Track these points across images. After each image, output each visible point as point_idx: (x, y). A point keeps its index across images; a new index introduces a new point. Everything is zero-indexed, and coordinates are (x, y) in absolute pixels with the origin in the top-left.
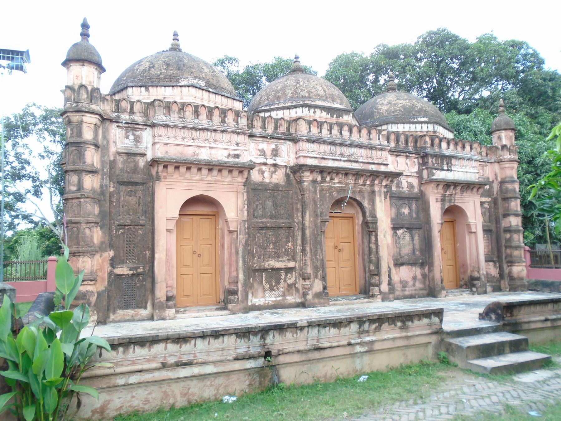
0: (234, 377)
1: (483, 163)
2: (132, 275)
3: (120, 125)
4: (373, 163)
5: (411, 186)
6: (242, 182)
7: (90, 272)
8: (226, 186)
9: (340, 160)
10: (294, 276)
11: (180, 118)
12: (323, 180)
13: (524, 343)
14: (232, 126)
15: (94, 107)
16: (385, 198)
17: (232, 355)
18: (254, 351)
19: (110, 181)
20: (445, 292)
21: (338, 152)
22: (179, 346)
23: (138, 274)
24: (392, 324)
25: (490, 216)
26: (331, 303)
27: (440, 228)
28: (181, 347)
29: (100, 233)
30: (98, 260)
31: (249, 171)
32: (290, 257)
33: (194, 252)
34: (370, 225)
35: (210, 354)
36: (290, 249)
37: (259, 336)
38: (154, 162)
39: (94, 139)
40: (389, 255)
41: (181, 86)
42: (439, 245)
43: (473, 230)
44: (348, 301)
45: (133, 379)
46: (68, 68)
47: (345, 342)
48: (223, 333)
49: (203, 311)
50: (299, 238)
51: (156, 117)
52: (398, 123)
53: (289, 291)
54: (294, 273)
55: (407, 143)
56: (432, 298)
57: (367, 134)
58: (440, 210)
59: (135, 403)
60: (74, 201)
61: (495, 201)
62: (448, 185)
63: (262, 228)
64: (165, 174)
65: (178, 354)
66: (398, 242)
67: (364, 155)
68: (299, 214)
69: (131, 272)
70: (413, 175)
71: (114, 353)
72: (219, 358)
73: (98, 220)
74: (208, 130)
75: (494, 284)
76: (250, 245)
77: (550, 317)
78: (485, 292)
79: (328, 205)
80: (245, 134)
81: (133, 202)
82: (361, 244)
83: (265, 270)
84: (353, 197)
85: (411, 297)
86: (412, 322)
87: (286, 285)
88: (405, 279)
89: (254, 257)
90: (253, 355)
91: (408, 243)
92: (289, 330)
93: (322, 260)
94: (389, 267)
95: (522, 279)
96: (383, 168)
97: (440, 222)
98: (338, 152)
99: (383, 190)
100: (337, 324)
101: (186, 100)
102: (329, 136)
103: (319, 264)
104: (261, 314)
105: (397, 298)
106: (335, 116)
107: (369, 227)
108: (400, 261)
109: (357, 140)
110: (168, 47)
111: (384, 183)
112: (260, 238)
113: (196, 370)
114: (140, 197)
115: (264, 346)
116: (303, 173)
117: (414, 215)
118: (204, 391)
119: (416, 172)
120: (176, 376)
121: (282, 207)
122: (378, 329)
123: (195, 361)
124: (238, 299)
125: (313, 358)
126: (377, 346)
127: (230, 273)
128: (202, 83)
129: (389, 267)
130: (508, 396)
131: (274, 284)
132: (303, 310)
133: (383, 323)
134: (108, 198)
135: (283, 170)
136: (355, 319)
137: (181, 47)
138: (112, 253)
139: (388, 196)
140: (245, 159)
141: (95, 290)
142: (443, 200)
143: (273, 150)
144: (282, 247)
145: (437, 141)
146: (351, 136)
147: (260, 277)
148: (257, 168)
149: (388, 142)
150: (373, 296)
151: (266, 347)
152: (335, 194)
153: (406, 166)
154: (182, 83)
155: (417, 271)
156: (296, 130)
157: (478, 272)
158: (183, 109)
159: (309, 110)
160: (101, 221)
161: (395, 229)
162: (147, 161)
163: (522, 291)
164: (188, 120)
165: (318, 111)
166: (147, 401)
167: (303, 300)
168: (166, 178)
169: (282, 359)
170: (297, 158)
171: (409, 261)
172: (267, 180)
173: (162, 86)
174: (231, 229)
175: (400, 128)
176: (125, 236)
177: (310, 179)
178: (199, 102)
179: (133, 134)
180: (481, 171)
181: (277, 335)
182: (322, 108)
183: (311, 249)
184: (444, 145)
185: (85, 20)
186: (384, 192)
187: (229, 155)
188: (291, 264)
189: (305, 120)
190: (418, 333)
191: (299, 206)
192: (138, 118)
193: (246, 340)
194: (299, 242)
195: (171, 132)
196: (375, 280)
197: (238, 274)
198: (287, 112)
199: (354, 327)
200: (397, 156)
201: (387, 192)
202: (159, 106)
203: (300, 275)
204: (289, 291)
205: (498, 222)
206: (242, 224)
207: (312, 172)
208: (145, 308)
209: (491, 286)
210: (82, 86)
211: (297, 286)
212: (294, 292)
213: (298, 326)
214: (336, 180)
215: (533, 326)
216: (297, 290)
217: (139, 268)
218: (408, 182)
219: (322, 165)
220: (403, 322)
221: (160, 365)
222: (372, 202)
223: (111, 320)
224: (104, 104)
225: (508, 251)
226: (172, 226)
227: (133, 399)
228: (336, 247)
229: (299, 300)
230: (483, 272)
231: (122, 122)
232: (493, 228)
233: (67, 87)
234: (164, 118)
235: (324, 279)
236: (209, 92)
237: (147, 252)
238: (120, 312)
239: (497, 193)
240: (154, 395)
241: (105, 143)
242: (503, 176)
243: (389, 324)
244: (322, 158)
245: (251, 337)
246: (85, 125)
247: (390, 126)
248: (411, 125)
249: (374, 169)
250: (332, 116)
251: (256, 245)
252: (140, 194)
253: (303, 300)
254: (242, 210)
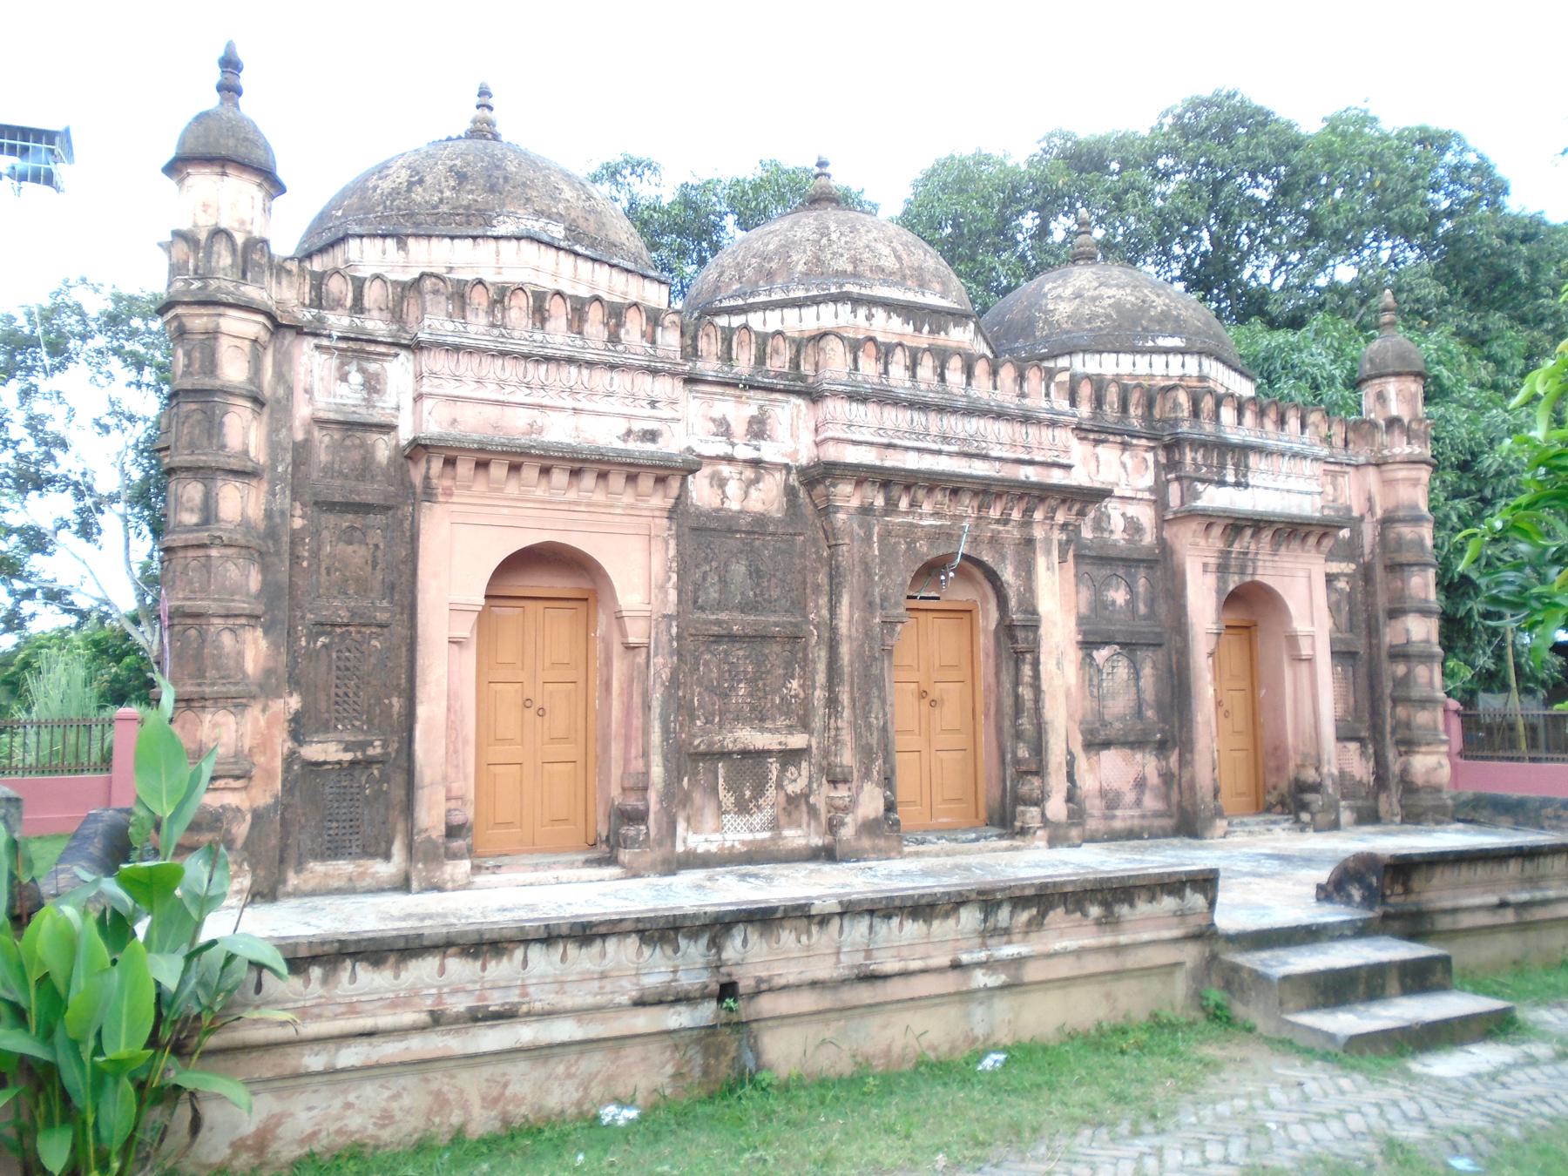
0: (632, 1053)
1: (1336, 466)
2: (353, 763)
3: (325, 342)
4: (1031, 463)
5: (1133, 526)
6: (662, 509)
7: (232, 753)
8: (618, 519)
9: (939, 452)
10: (805, 773)
11: (493, 326)
12: (891, 507)
13: (1439, 966)
14: (639, 350)
15: (251, 292)
16: (1063, 560)
17: (627, 991)
18: (691, 979)
19: (294, 499)
20: (1224, 823)
21: (934, 430)
22: (479, 964)
23: (369, 762)
24: (1074, 912)
25: (1351, 612)
26: (906, 849)
27: (1212, 646)
28: (484, 968)
29: (263, 644)
30: (256, 720)
31: (684, 479)
32: (794, 720)
33: (527, 703)
34: (1020, 634)
35: (567, 987)
36: (796, 696)
37: (704, 941)
38: (418, 449)
39: (250, 381)
40: (1070, 717)
41: (496, 238)
42: (1210, 691)
43: (1305, 651)
44: (953, 845)
45: (350, 1056)
46: (181, 182)
47: (945, 960)
48: (603, 930)
49: (550, 866)
50: (821, 667)
51: (427, 322)
52: (1100, 352)
53: (789, 815)
54: (804, 765)
55: (1124, 407)
56: (1188, 841)
57: (1015, 380)
59: (354, 1122)
60: (191, 553)
61: (1366, 573)
62: (1237, 525)
63: (718, 639)
64: (447, 483)
65: (478, 986)
66: (1095, 682)
67: (1005, 439)
68: (823, 601)
69: (348, 756)
70: (1139, 495)
71: (296, 982)
72: (590, 1000)
73: (259, 609)
74: (570, 361)
75: (1360, 803)
76: (685, 684)
77: (1512, 898)
78: (1335, 826)
79: (903, 574)
80: (673, 375)
81: (357, 560)
82: (993, 687)
83: (724, 755)
84: (973, 554)
85: (1131, 835)
86: (1132, 905)
87: (782, 799)
88: (1115, 786)
89: (692, 717)
90: (688, 992)
91: (1124, 684)
92: (786, 923)
93: (884, 730)
94: (1069, 752)
95: (1437, 790)
96: (1056, 477)
97: (1213, 628)
98: (934, 430)
99: (1057, 536)
100: (922, 909)
101: (512, 276)
102: (908, 384)
103: (874, 740)
104: (710, 879)
105: (1092, 839)
106: (926, 328)
107: (1017, 639)
108: (1102, 736)
109: (985, 396)
110: (463, 126)
111: (1060, 517)
112: (711, 665)
113: (526, 1033)
114: (377, 546)
115: (718, 967)
116: (835, 486)
117: (1142, 609)
118: (548, 1092)
119: (1150, 490)
120: (471, 1050)
121: (774, 580)
122: (1036, 924)
123: (524, 1008)
124: (647, 834)
125: (855, 1002)
126: (1032, 973)
127: (627, 761)
128: (557, 231)
129: (1069, 752)
130: (1393, 1114)
131: (748, 793)
132: (827, 868)
133: (1051, 907)
134: (286, 548)
135: (778, 475)
136: (974, 896)
137: (498, 129)
138: (295, 702)
139: (1071, 553)
140: (672, 444)
141: (245, 806)
142: (1223, 569)
143: (753, 421)
144: (774, 692)
145: (1207, 403)
146: (969, 384)
147: (710, 776)
148: (706, 471)
149: (1073, 403)
150: (1023, 832)
151: (723, 970)
152: (923, 547)
153: (1123, 471)
154: (500, 230)
155: (1148, 764)
156: (817, 364)
157: (1317, 769)
158: (501, 301)
159: (854, 311)
160: (265, 613)
161: (1088, 645)
162: (397, 445)
163: (1438, 823)
164: (516, 334)
165: (880, 313)
166: (386, 1118)
167: (828, 839)
168: (451, 495)
169: (767, 1005)
170: (817, 444)
171: (1125, 735)
172: (734, 505)
173: (444, 236)
174: (632, 640)
175: (1107, 365)
176: (334, 655)
177: (855, 502)
178: (548, 284)
179: (361, 370)
180: (1329, 489)
181: (754, 937)
182: (890, 306)
183: (853, 700)
184: (1228, 415)
185: (230, 47)
187: (629, 432)
188: (797, 741)
189: (842, 338)
190: (1145, 937)
191: (822, 578)
192: (376, 325)
193: (669, 951)
194: (821, 678)
195: (466, 364)
196: (1031, 786)
197: (647, 765)
198: (791, 314)
199: (970, 917)
200: (1097, 442)
201: (1068, 542)
202: (436, 292)
203: (821, 769)
204: (789, 815)
205: (1373, 631)
206: (663, 626)
207: (859, 483)
208: (387, 856)
209: (1350, 808)
210: (218, 233)
211: (812, 800)
212: (805, 818)
213: (813, 912)
214: (927, 507)
215: (1466, 921)
216: (813, 811)
217: (371, 744)
218: (1128, 516)
219: (888, 464)
220: (1107, 905)
221: (424, 1018)
222: (1026, 569)
223: (289, 888)
224: (279, 283)
225: (1401, 712)
226: (465, 628)
227: (349, 1112)
228: (923, 694)
229: (817, 841)
230: (1331, 769)
231: (329, 336)
232: (1361, 646)
233: (177, 234)
234: (449, 326)
235: (888, 781)
236: (576, 254)
237: (395, 700)
238: (317, 867)
239: (1372, 552)
240: (406, 1101)
241: (281, 392)
242: (1391, 504)
243: (1067, 912)
244: (890, 446)
245: (683, 942)
246: (224, 344)
247: (1078, 360)
248: (1138, 357)
249: (1033, 479)
250: (918, 330)
251: (700, 684)
252: (376, 536)
253: (828, 839)
254: (662, 588)
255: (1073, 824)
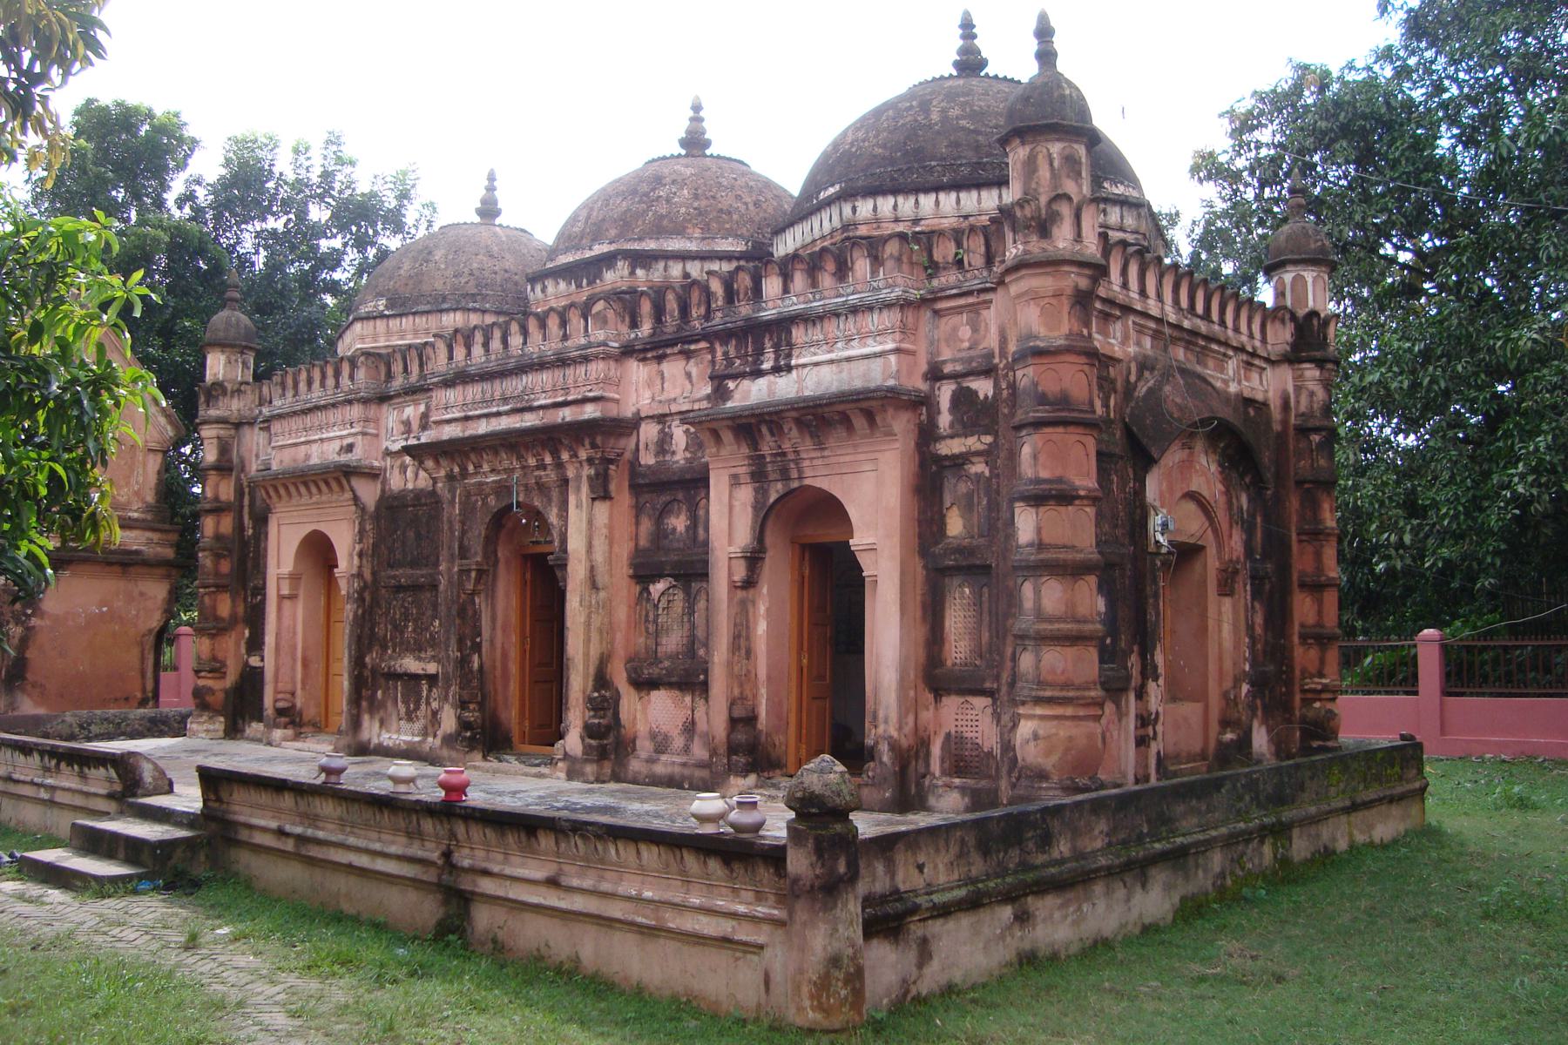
4: (565, 404)
9: (498, 414)
58: (750, 509)
66: (651, 617)
77: (288, 828)
88: (664, 729)
98: (497, 395)
99: (588, 471)
111: (583, 455)
142: (759, 476)
144: (427, 629)
146: (525, 343)
152: (492, 500)
186: (589, 477)
200: (660, 359)
214: (486, 468)
215: (259, 838)
219: (467, 433)
244: (467, 418)
255: (586, 761)
